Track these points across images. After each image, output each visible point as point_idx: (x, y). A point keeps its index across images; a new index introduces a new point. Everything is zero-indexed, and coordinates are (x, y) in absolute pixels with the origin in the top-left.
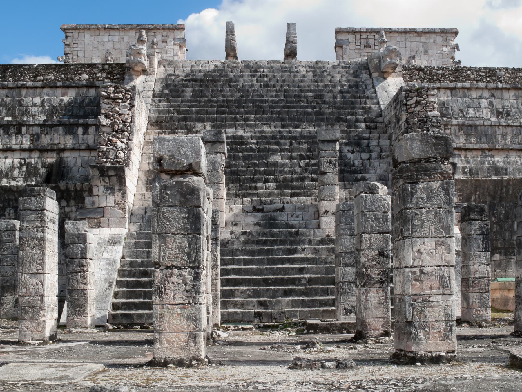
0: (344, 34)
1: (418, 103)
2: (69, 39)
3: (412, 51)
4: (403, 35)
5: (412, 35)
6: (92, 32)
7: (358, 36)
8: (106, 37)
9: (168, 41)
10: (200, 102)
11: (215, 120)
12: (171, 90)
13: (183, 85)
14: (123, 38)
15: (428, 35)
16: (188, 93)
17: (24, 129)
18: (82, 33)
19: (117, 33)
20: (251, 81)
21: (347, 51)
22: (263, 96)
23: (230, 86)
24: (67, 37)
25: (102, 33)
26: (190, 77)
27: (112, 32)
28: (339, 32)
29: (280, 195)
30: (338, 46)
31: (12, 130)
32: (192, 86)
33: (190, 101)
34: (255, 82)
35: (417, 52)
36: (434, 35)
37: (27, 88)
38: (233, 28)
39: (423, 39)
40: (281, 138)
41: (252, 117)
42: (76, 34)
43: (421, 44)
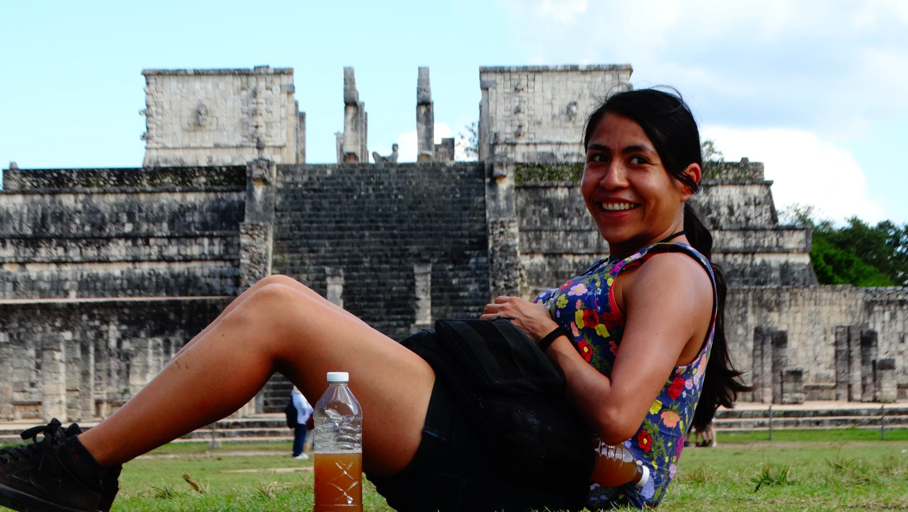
0: (490, 75)
1: (501, 233)
2: (152, 87)
3: (574, 93)
4: (564, 74)
5: (574, 73)
6: (180, 78)
7: (507, 76)
8: (197, 84)
9: (274, 88)
10: (318, 216)
11: (334, 237)
12: (291, 203)
13: (303, 196)
14: (217, 86)
15: (594, 73)
16: (308, 207)
17: (152, 241)
18: (167, 80)
19: (210, 79)
20: (367, 190)
21: (494, 95)
22: (377, 209)
23: (347, 197)
24: (148, 83)
25: (192, 79)
26: (309, 187)
27: (204, 78)
28: (484, 71)
29: (388, 313)
30: (485, 88)
31: (140, 242)
32: (311, 198)
33: (310, 216)
34: (371, 191)
35: (580, 96)
36: (602, 73)
37: (145, 192)
38: (352, 74)
39: (588, 78)
40: (392, 256)
41: (367, 233)
42: (159, 79)
43: (585, 85)
